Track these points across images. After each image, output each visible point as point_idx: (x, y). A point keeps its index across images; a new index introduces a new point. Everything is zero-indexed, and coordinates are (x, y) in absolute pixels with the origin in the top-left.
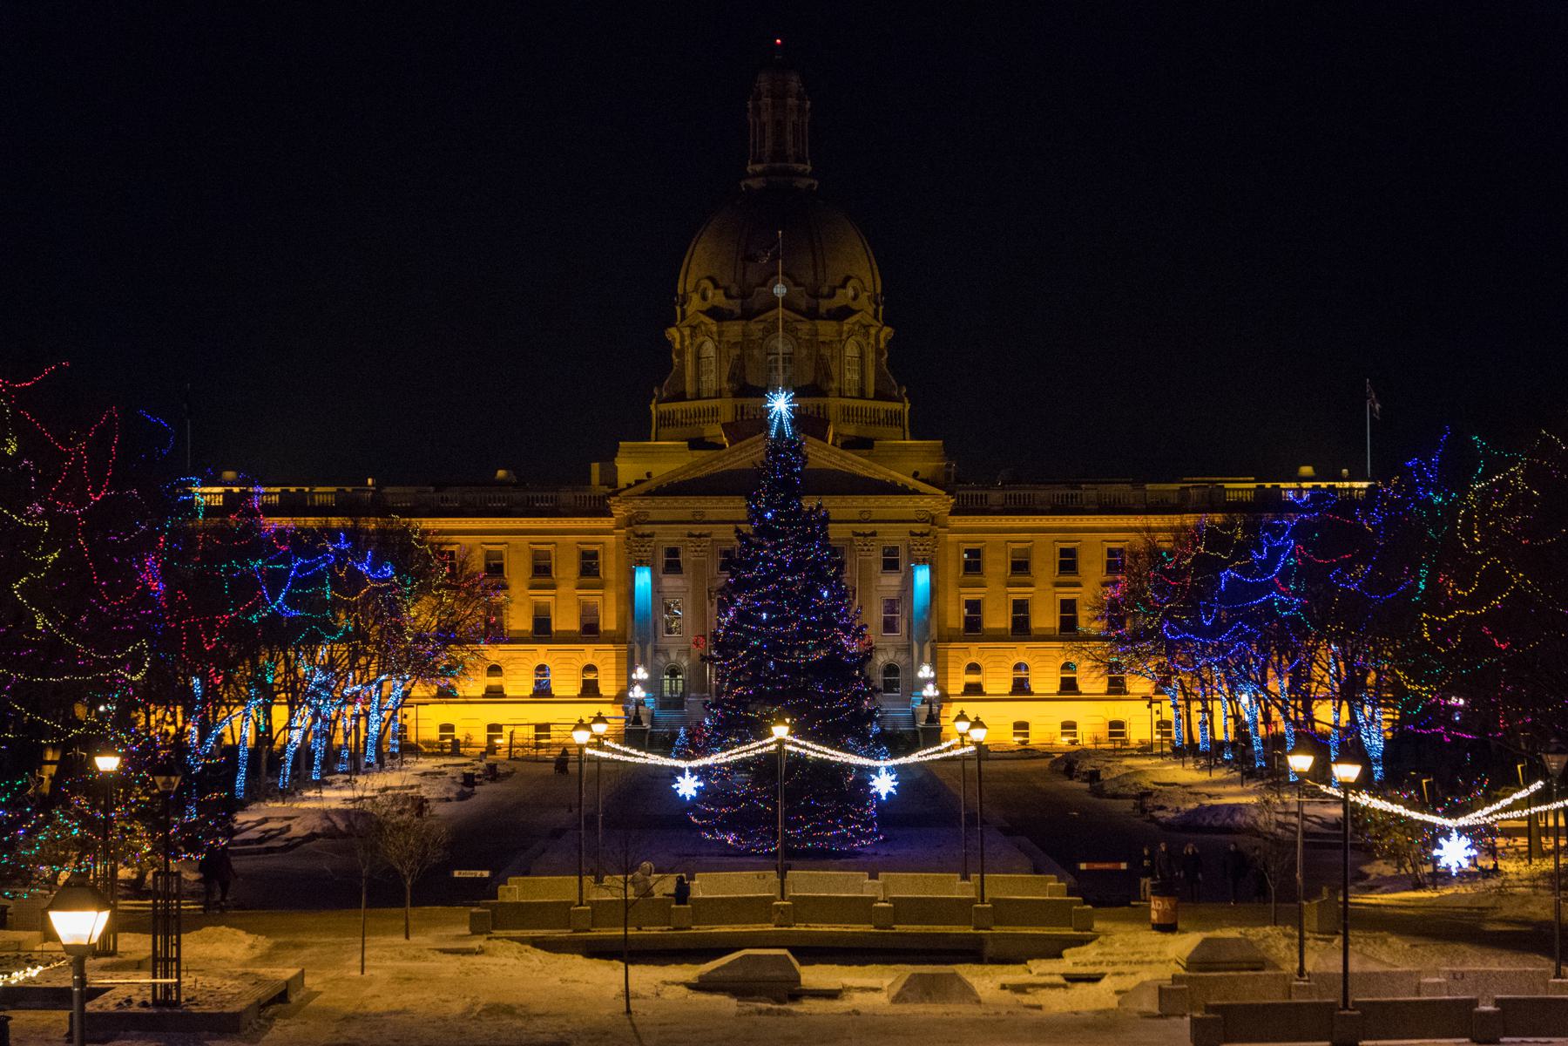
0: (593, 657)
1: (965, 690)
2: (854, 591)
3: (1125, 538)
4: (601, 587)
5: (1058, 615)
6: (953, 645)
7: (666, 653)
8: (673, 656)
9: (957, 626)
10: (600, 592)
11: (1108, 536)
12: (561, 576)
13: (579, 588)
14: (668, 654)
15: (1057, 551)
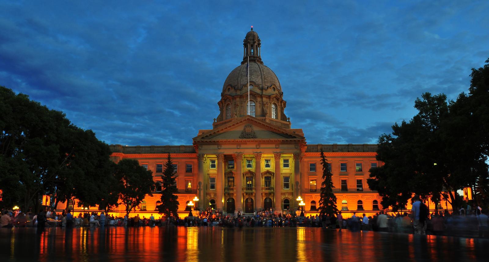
0: (189, 198)
1: (311, 209)
2: (274, 174)
3: (361, 160)
4: (193, 176)
5: (341, 185)
6: (307, 194)
7: (210, 196)
8: (212, 196)
9: (308, 188)
10: (192, 177)
11: (356, 159)
12: (180, 172)
13: (185, 176)
14: (211, 196)
15: (340, 164)
